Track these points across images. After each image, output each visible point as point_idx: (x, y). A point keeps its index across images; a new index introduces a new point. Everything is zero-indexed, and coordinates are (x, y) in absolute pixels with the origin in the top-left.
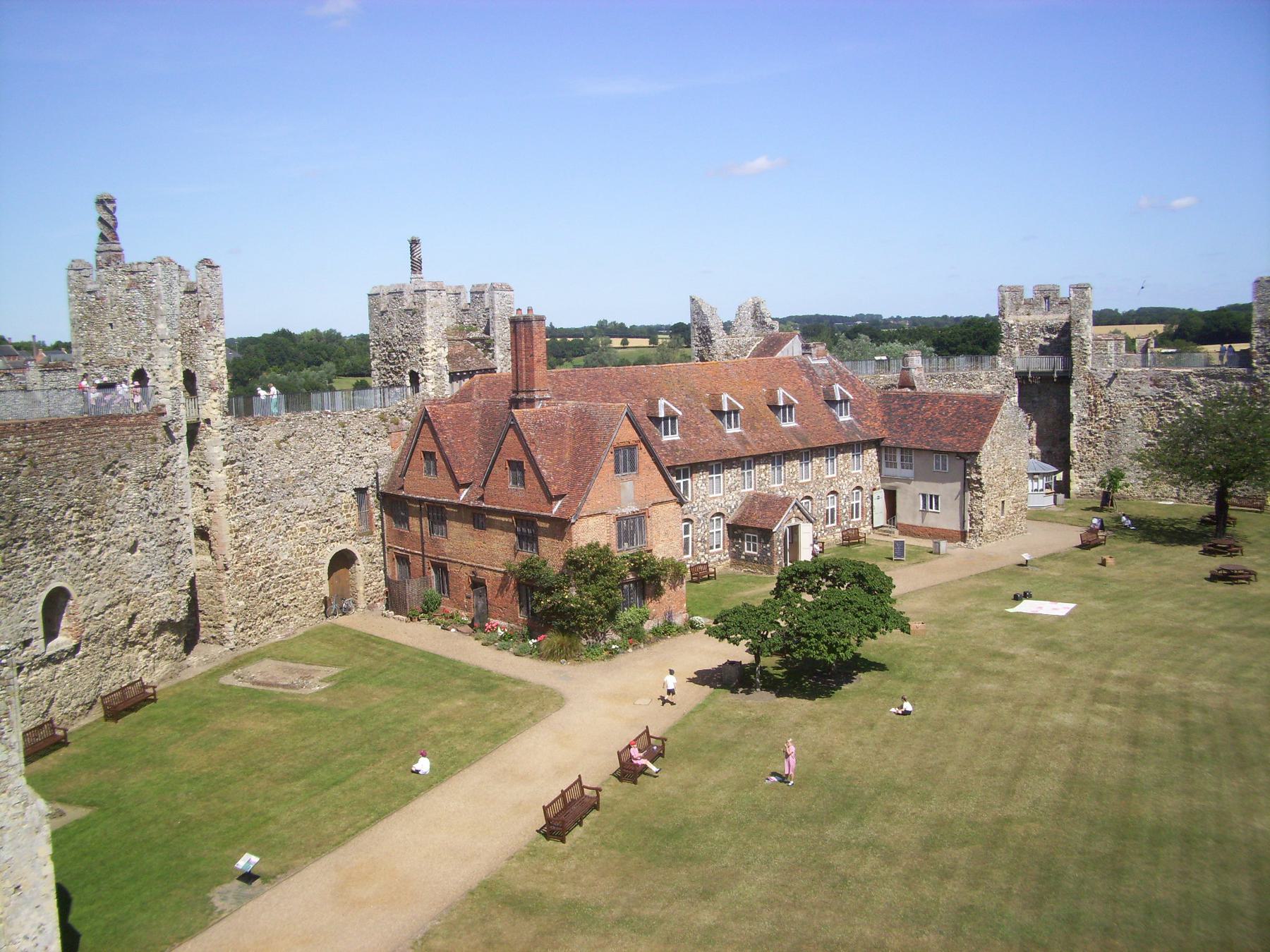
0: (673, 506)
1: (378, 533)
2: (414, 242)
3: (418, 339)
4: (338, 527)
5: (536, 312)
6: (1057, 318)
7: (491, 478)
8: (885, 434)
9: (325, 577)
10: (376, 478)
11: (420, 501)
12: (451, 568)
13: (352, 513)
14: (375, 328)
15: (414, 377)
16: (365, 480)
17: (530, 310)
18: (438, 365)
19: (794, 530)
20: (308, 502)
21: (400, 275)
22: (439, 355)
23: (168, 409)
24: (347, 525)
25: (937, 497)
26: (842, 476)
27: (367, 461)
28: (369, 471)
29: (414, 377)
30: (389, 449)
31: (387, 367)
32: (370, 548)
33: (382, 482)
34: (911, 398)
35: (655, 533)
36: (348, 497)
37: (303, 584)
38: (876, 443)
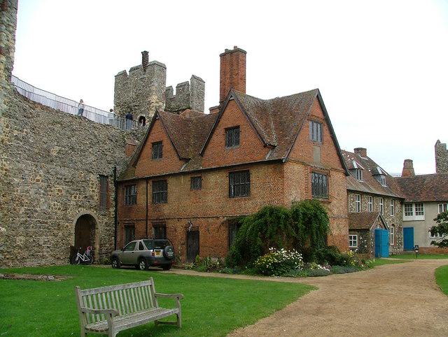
0: (341, 175)
1: (112, 210)
3: (148, 95)
4: (86, 197)
7: (210, 146)
10: (115, 171)
11: (147, 180)
12: (170, 224)
13: (96, 190)
16: (108, 171)
20: (65, 171)
24: (92, 197)
27: (109, 159)
33: (118, 175)
36: (94, 178)
37: (56, 232)
38: (402, 201)
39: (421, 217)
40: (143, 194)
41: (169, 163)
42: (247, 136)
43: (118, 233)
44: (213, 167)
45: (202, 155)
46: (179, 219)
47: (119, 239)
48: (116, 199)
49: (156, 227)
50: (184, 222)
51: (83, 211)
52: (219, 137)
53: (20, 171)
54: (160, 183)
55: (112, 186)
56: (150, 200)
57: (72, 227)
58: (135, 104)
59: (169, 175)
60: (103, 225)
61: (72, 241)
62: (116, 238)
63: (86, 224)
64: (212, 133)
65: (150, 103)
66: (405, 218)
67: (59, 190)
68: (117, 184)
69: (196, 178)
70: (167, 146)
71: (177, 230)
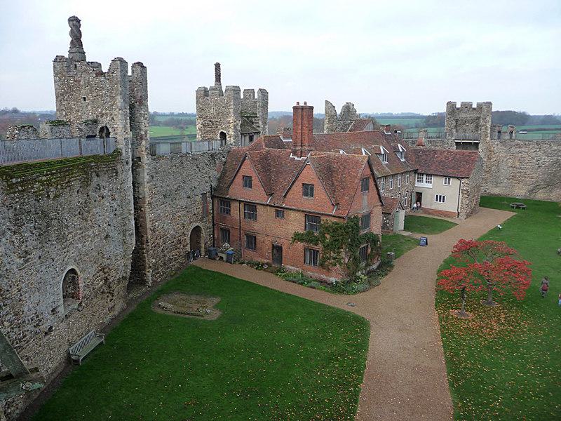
1: (210, 216)
2: (218, 66)
5: (308, 105)
6: (475, 115)
8: (418, 167)
11: (240, 202)
12: (259, 238)
14: (200, 109)
15: (223, 135)
17: (305, 103)
18: (237, 130)
21: (210, 83)
22: (237, 124)
23: (124, 151)
25: (444, 197)
26: (402, 186)
28: (207, 184)
29: (223, 135)
30: (216, 173)
31: (207, 129)
34: (422, 150)
36: (199, 198)
38: (416, 172)
39: (430, 186)
40: (236, 211)
41: (257, 194)
42: (319, 190)
43: (216, 232)
44: (294, 208)
45: (285, 196)
47: (216, 236)
48: (213, 209)
49: (248, 236)
50: (270, 238)
52: (298, 188)
54: (251, 208)
55: (209, 199)
56: (242, 216)
58: (216, 119)
59: (258, 204)
60: (205, 227)
61: (188, 248)
62: (213, 236)
64: (293, 184)
65: (229, 123)
66: (417, 184)
67: (179, 217)
68: (213, 197)
69: (280, 212)
70: (256, 181)
71: (265, 243)
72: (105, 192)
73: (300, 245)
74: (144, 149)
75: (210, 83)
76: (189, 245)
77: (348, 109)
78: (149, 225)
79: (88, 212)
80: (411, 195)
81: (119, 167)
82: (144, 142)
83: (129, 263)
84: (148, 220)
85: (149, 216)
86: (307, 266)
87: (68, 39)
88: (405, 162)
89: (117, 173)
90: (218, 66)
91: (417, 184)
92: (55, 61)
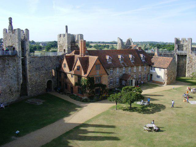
0: (106, 75)
2: (67, 27)
9: (46, 85)
19: (132, 80)
22: (69, 46)
27: (55, 65)
32: (55, 80)
35: (103, 80)
46: (69, 84)
51: (49, 79)
53: (33, 75)
57: (46, 84)
61: (46, 87)
63: (49, 83)
72: (11, 66)
73: (77, 87)
74: (27, 54)
75: (64, 32)
76: (46, 86)
77: (129, 41)
78: (28, 77)
79: (4, 70)
80: (148, 75)
81: (16, 59)
82: (27, 52)
83: (20, 87)
84: (28, 75)
85: (29, 74)
86: (79, 94)
87: (9, 24)
88: (144, 62)
89: (15, 60)
90: (67, 27)
91: (151, 71)
92: (4, 30)
